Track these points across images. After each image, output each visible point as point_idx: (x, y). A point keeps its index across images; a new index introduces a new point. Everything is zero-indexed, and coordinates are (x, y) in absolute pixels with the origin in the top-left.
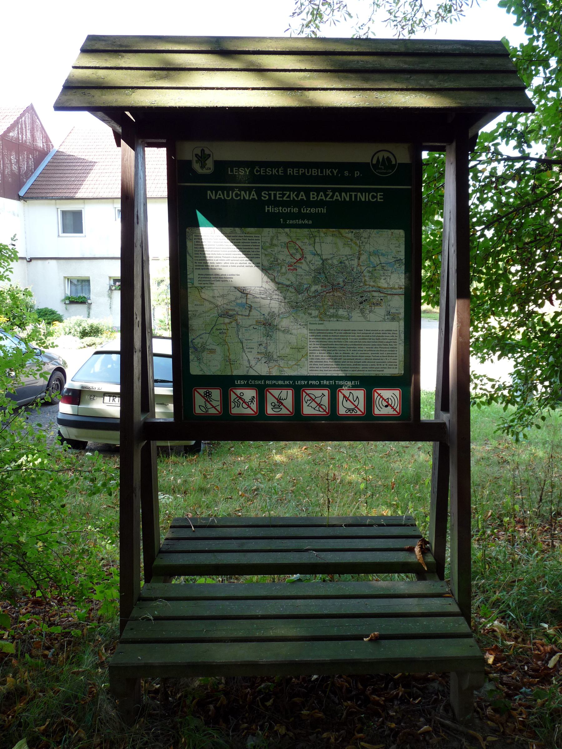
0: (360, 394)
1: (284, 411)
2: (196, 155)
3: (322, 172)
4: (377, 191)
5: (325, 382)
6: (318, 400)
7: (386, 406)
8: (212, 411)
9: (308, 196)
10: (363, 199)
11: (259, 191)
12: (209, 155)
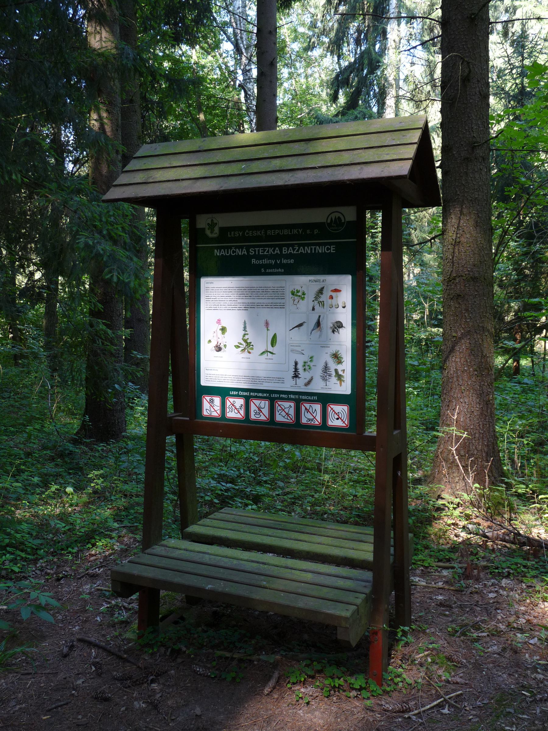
0: (318, 407)
1: (263, 418)
3: (291, 232)
4: (331, 244)
5: (292, 396)
6: (287, 410)
7: (337, 419)
8: (214, 414)
9: (281, 251)
10: (320, 251)
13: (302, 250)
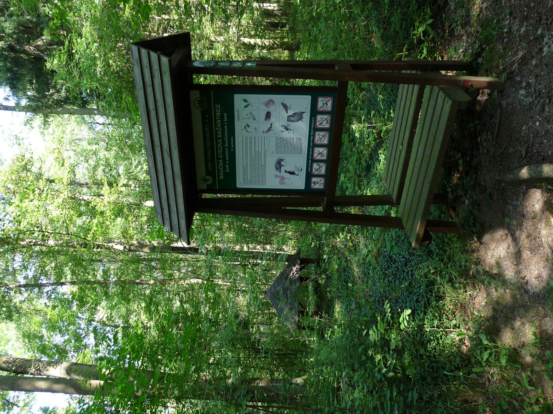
0: (319, 117)
1: (325, 152)
4: (215, 107)
5: (312, 133)
6: (321, 137)
8: (323, 181)
9: (220, 138)
11: (218, 159)
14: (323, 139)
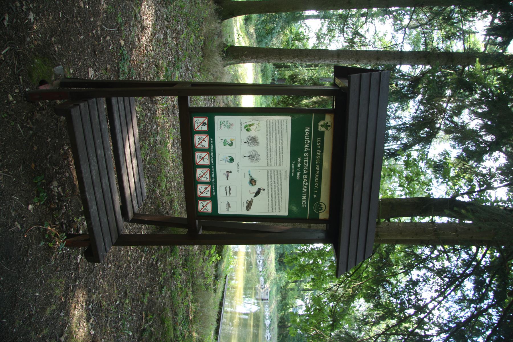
0: (209, 195)
1: (198, 161)
2: (327, 123)
4: (307, 204)
5: (213, 180)
6: (204, 176)
8: (196, 126)
9: (305, 174)
11: (309, 152)
12: (327, 129)
13: (305, 187)
14: (202, 174)
